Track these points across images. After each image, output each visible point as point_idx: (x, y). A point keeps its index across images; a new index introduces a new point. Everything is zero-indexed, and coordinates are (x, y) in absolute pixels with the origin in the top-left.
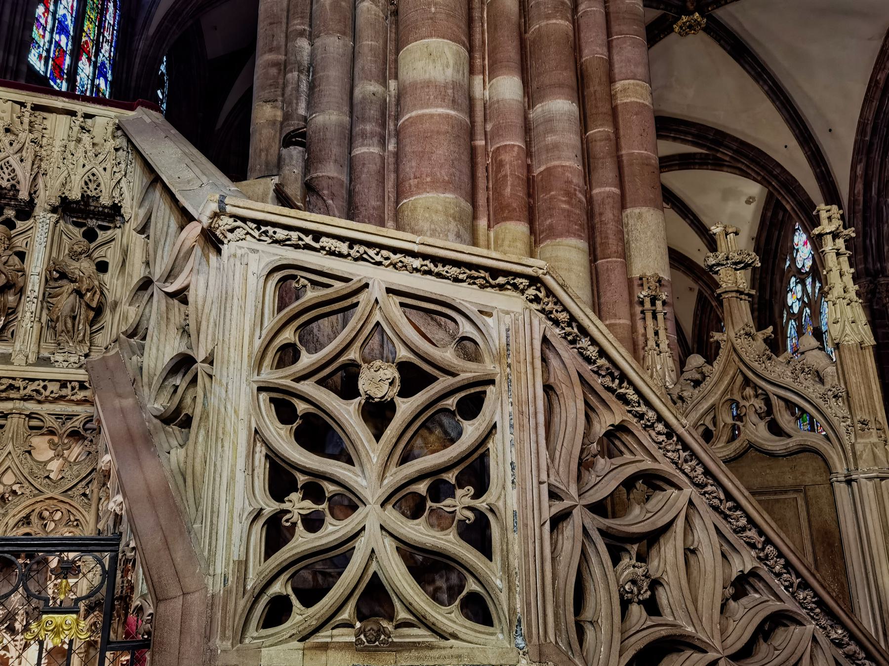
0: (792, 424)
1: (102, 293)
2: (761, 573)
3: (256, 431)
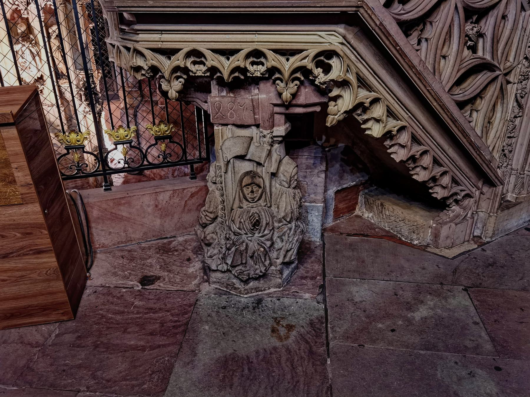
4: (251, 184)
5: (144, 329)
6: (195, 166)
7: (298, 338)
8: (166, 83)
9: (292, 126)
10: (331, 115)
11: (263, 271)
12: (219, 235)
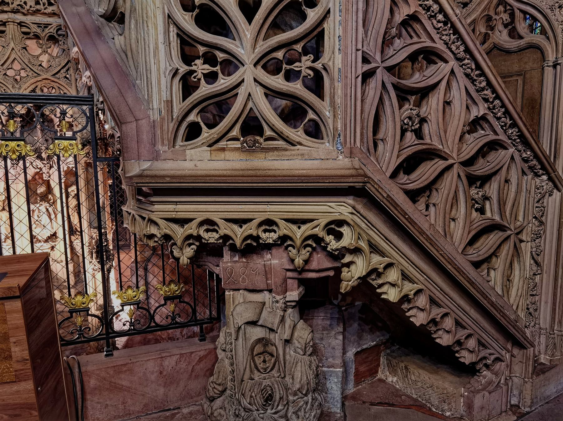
4: (263, 352)
9: (306, 290)
10: (345, 281)
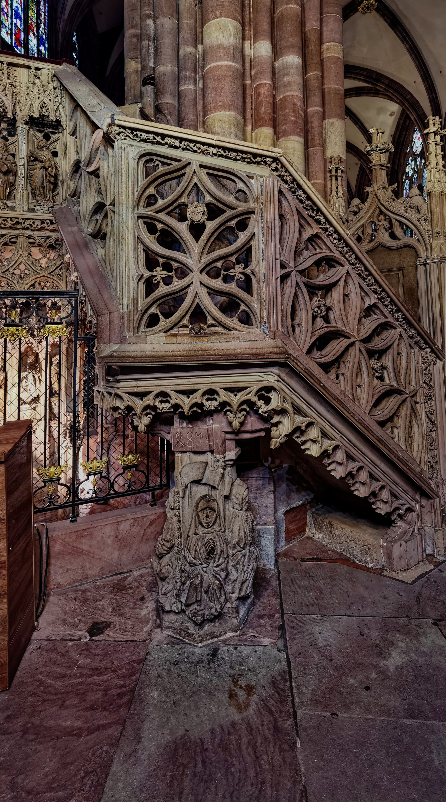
0: (402, 234)
1: (56, 168)
2: (379, 305)
3: (138, 238)
5: (84, 701)
6: (156, 492)
7: (260, 707)
8: (137, 419)
9: (242, 450)
11: (219, 610)
12: (174, 568)
